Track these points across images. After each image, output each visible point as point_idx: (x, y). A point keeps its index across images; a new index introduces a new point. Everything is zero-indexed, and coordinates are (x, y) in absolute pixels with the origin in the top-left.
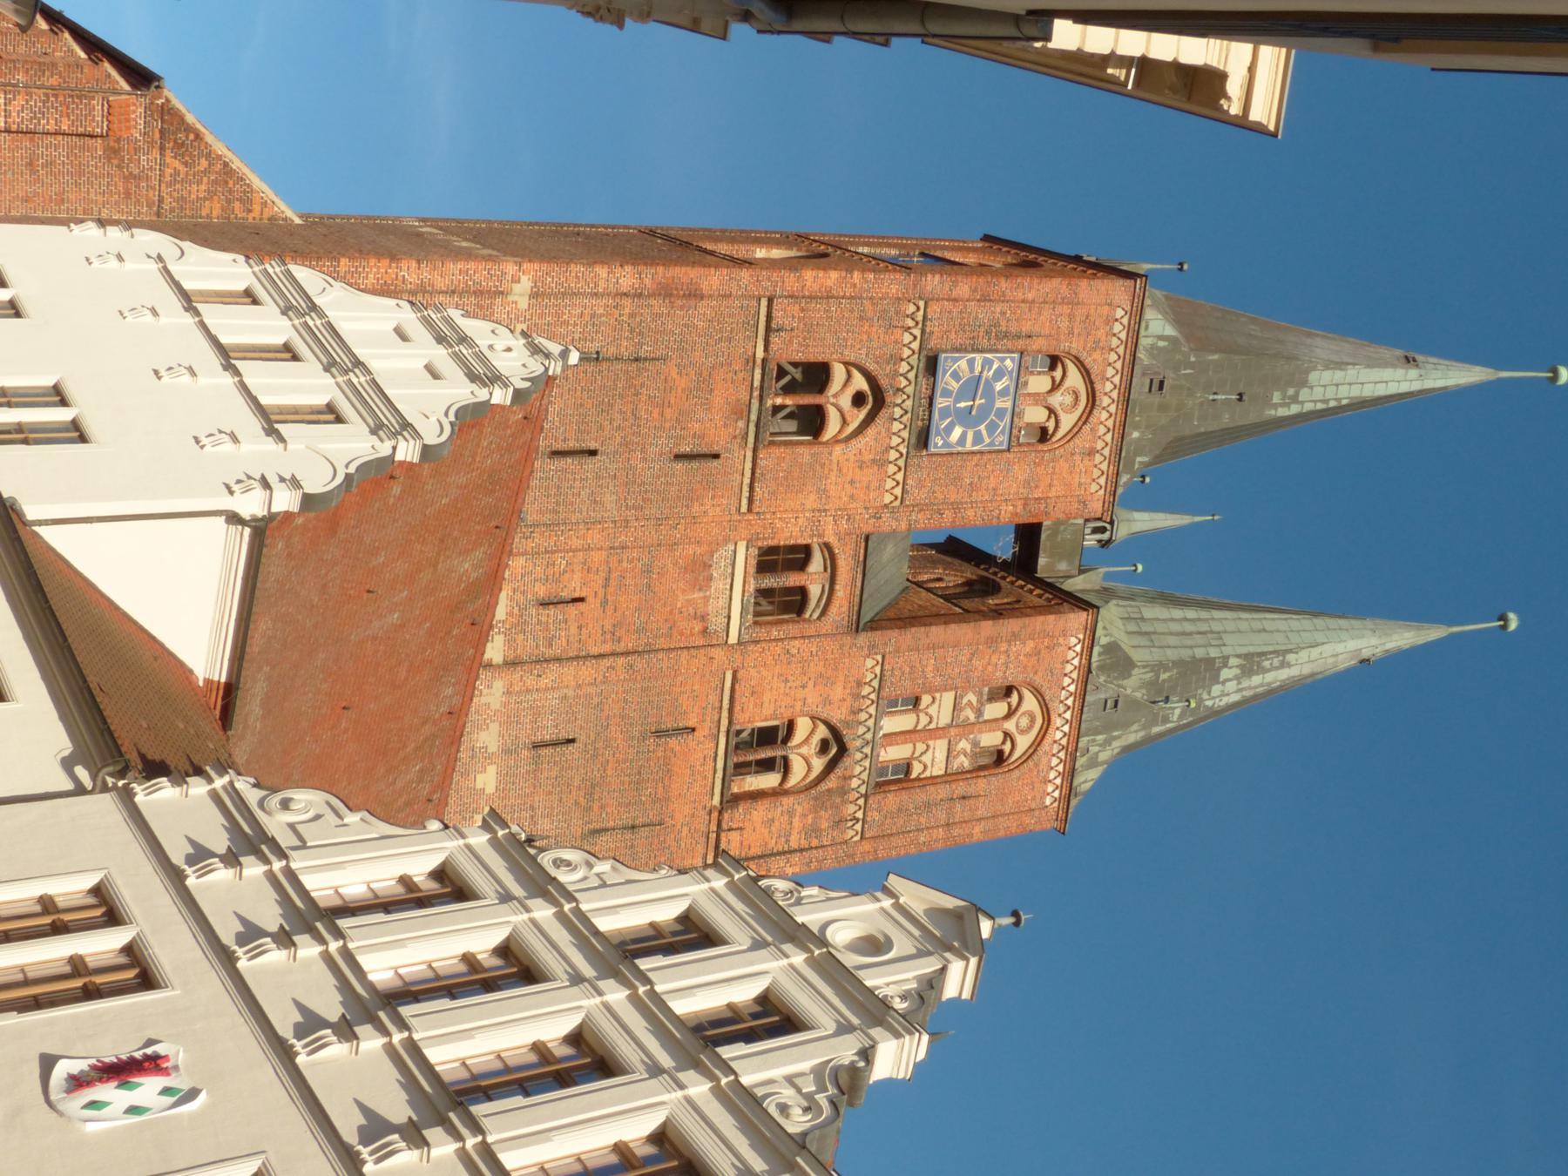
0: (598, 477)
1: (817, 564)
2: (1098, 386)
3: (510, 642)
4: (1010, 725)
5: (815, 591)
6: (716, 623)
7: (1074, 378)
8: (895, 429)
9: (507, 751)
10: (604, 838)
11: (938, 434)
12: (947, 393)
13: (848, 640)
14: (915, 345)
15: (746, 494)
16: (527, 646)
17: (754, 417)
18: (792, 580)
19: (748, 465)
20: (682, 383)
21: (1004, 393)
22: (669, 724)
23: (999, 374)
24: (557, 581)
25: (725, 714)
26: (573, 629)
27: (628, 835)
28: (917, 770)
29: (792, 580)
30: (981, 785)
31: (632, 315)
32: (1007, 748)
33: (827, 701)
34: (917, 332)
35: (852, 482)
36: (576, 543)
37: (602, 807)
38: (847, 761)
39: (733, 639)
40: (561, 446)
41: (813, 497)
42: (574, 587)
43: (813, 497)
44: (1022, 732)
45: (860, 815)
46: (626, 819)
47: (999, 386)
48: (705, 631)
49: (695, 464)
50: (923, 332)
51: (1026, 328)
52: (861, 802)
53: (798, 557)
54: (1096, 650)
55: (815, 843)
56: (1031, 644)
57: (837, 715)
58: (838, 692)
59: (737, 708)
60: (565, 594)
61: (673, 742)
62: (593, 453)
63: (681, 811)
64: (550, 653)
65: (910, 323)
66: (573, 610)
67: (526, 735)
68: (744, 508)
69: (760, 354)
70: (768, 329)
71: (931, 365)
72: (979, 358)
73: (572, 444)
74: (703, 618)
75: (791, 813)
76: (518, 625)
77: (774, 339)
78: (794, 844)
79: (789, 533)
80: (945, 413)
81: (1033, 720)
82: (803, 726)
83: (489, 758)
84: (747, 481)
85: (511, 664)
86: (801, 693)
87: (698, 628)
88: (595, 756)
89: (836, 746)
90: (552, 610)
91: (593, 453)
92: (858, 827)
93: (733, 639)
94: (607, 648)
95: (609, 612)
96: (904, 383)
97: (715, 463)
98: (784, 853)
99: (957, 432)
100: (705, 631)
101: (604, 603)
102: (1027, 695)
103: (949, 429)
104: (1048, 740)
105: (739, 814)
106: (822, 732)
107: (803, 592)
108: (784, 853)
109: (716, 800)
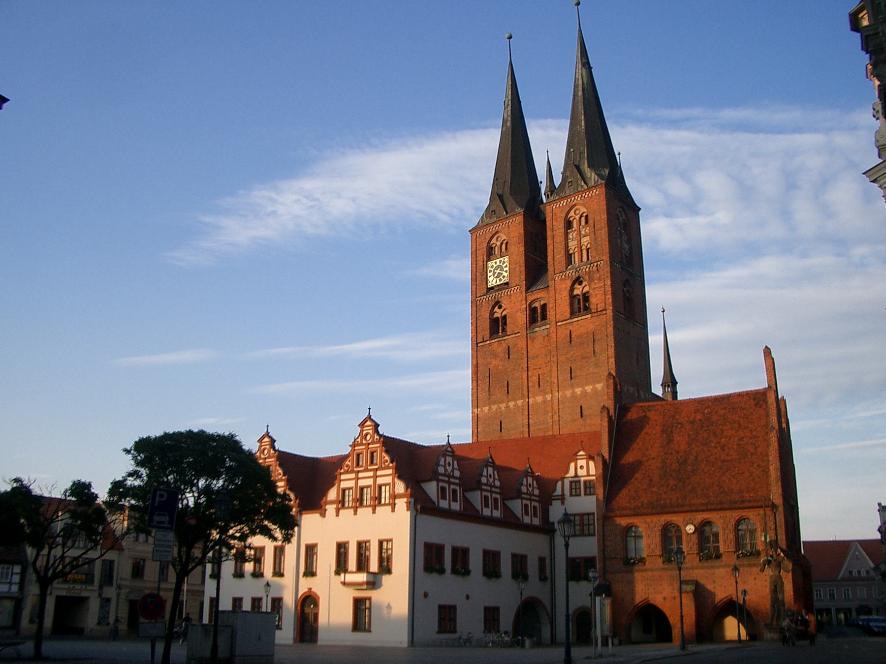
3: (547, 393)
4: (577, 217)
6: (546, 332)
7: (494, 241)
8: (503, 295)
9: (572, 386)
10: (596, 351)
20: (494, 362)
30: (591, 222)
42: (535, 379)
46: (591, 344)
53: (533, 311)
56: (555, 223)
57: (569, 283)
61: (573, 336)
63: (592, 326)
71: (492, 288)
72: (489, 275)
76: (544, 393)
78: (602, 284)
80: (500, 280)
82: (575, 293)
83: (574, 392)
89: (578, 281)
93: (548, 326)
105: (593, 307)
106: (576, 286)
109: (589, 316)
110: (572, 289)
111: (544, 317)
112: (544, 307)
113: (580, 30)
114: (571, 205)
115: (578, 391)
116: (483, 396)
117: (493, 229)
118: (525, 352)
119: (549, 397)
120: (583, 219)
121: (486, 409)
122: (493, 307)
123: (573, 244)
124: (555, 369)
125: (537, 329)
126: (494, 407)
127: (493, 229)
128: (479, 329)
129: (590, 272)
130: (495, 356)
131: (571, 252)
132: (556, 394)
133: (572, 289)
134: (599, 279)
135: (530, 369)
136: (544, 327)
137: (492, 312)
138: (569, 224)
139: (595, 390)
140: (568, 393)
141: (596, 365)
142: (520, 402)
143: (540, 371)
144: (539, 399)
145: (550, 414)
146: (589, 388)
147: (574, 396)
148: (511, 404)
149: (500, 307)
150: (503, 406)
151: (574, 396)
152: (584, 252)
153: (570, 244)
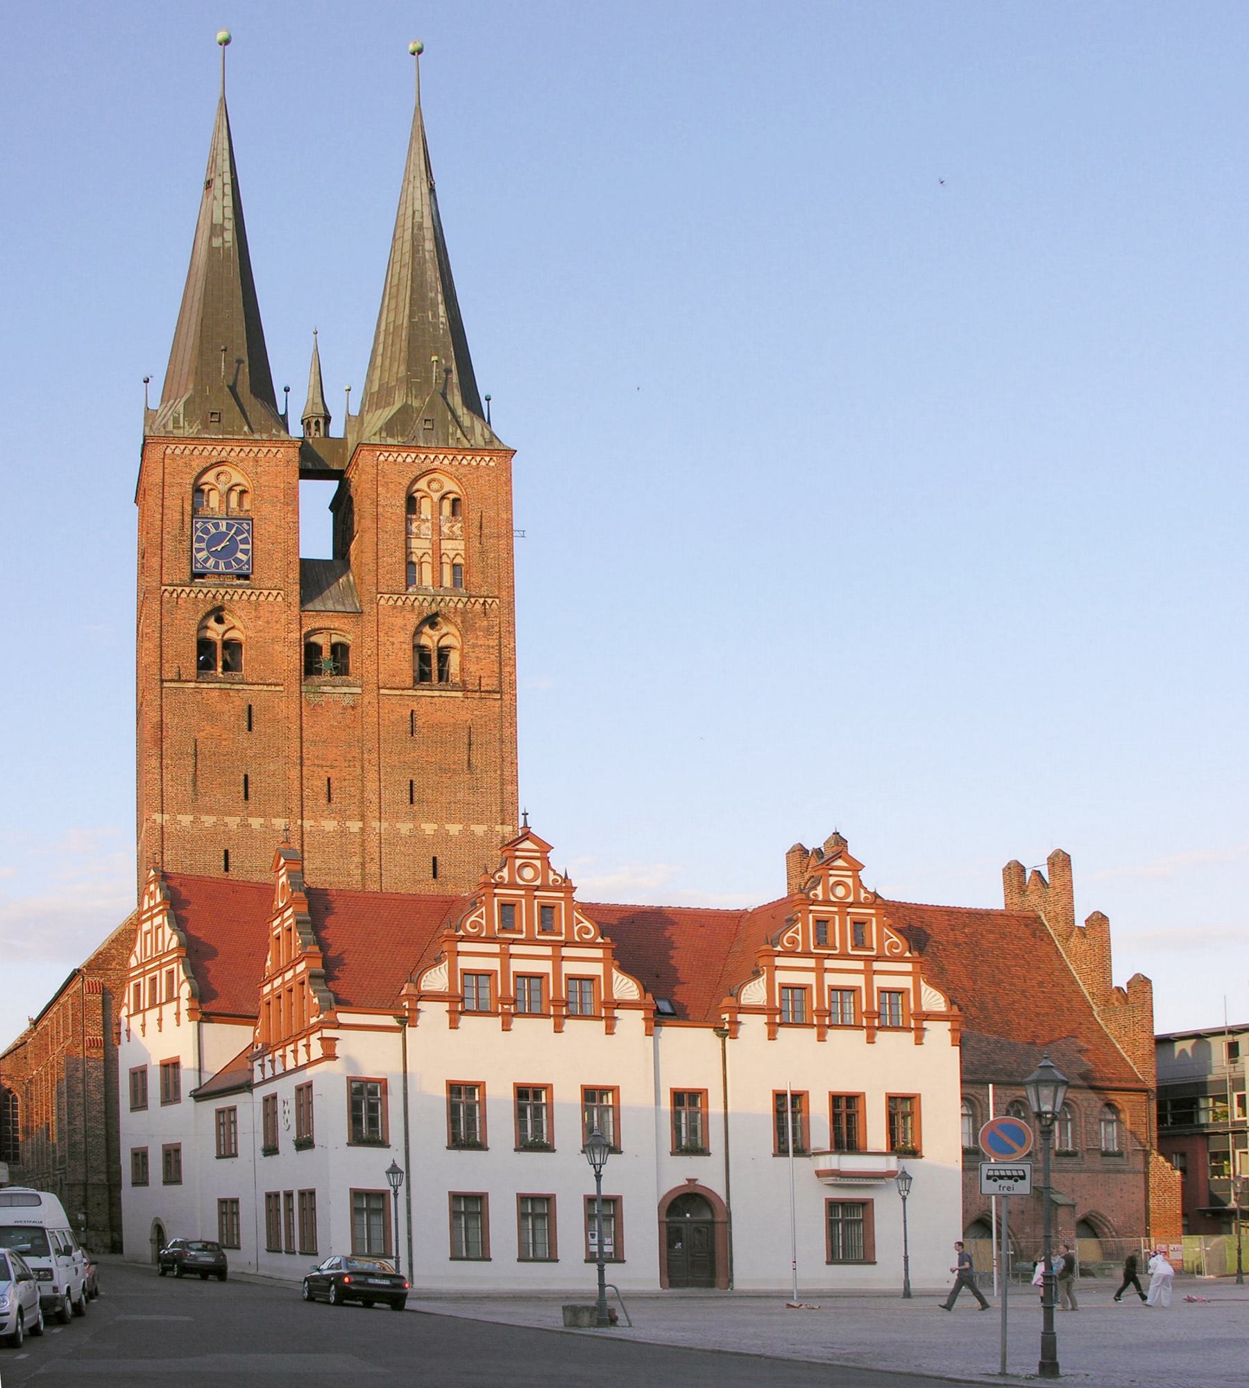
0: (260, 773)
1: (317, 639)
2: (214, 461)
3: (350, 818)
4: (436, 496)
5: (335, 639)
6: (348, 701)
8: (237, 597)
11: (241, 569)
12: (216, 565)
13: (365, 617)
14: (187, 590)
15: (273, 688)
16: (354, 809)
17: (228, 686)
18: (326, 653)
19: (256, 687)
21: (216, 526)
22: (408, 725)
23: (206, 531)
24: (317, 793)
25: (405, 692)
26: (346, 783)
27: (473, 747)
28: (459, 560)
29: (326, 653)
31: (172, 759)
32: (452, 496)
33: (404, 628)
34: (180, 589)
35: (268, 622)
36: (297, 784)
37: (454, 763)
38: (444, 611)
39: (358, 690)
40: (242, 794)
41: (276, 647)
42: (320, 785)
43: (276, 647)
44: (442, 487)
45: (482, 601)
47: (213, 531)
48: (353, 708)
49: (254, 719)
50: (181, 585)
51: (178, 516)
52: (473, 600)
53: (311, 651)
54: (390, 441)
55: (496, 629)
57: (413, 621)
58: (399, 621)
59: (403, 685)
60: (326, 789)
61: (419, 723)
62: (246, 776)
63: (464, 716)
64: (358, 797)
65: (175, 595)
66: (334, 785)
67: (405, 807)
68: (281, 688)
69: (192, 685)
70: (179, 680)
72: (196, 545)
73: (242, 788)
74: (345, 708)
75: (474, 646)
76: (343, 816)
77: (183, 678)
79: (294, 658)
80: (228, 565)
81: (434, 480)
84: (265, 688)
85: (363, 818)
86: (397, 646)
87: (350, 711)
88: (422, 769)
90: (334, 796)
91: (246, 776)
92: (489, 601)
93: (358, 690)
94: (358, 764)
95: (337, 764)
96: (210, 595)
97: (254, 707)
98: (500, 649)
99: (240, 555)
100: (353, 708)
101: (332, 767)
102: (416, 487)
103: (238, 561)
104: (449, 469)
106: (427, 629)
107: (335, 648)
108: (500, 649)
109: (460, 694)
110: (418, 632)
111: (341, 669)
112: (340, 651)
113: (418, 109)
114: (424, 467)
115: (429, 828)
116: (177, 789)
117: (217, 453)
118: (295, 727)
119: (355, 826)
120: (447, 505)
121: (186, 819)
122: (208, 615)
123: (420, 546)
124: (372, 775)
125: (326, 689)
126: (209, 820)
127: (217, 453)
128: (169, 653)
129: (464, 613)
130: (212, 717)
131: (415, 559)
132: (375, 824)
133: (418, 632)
134: (488, 631)
135: (306, 762)
136: (345, 690)
137: (203, 627)
138: (411, 504)
139: (468, 836)
140: (405, 828)
141: (474, 789)
142: (280, 823)
143: (333, 774)
144: (330, 825)
145: (357, 859)
146: (454, 829)
147: (416, 835)
148: (256, 822)
149: (220, 620)
150: (233, 822)
151: (416, 835)
152: (447, 570)
153: (415, 543)
